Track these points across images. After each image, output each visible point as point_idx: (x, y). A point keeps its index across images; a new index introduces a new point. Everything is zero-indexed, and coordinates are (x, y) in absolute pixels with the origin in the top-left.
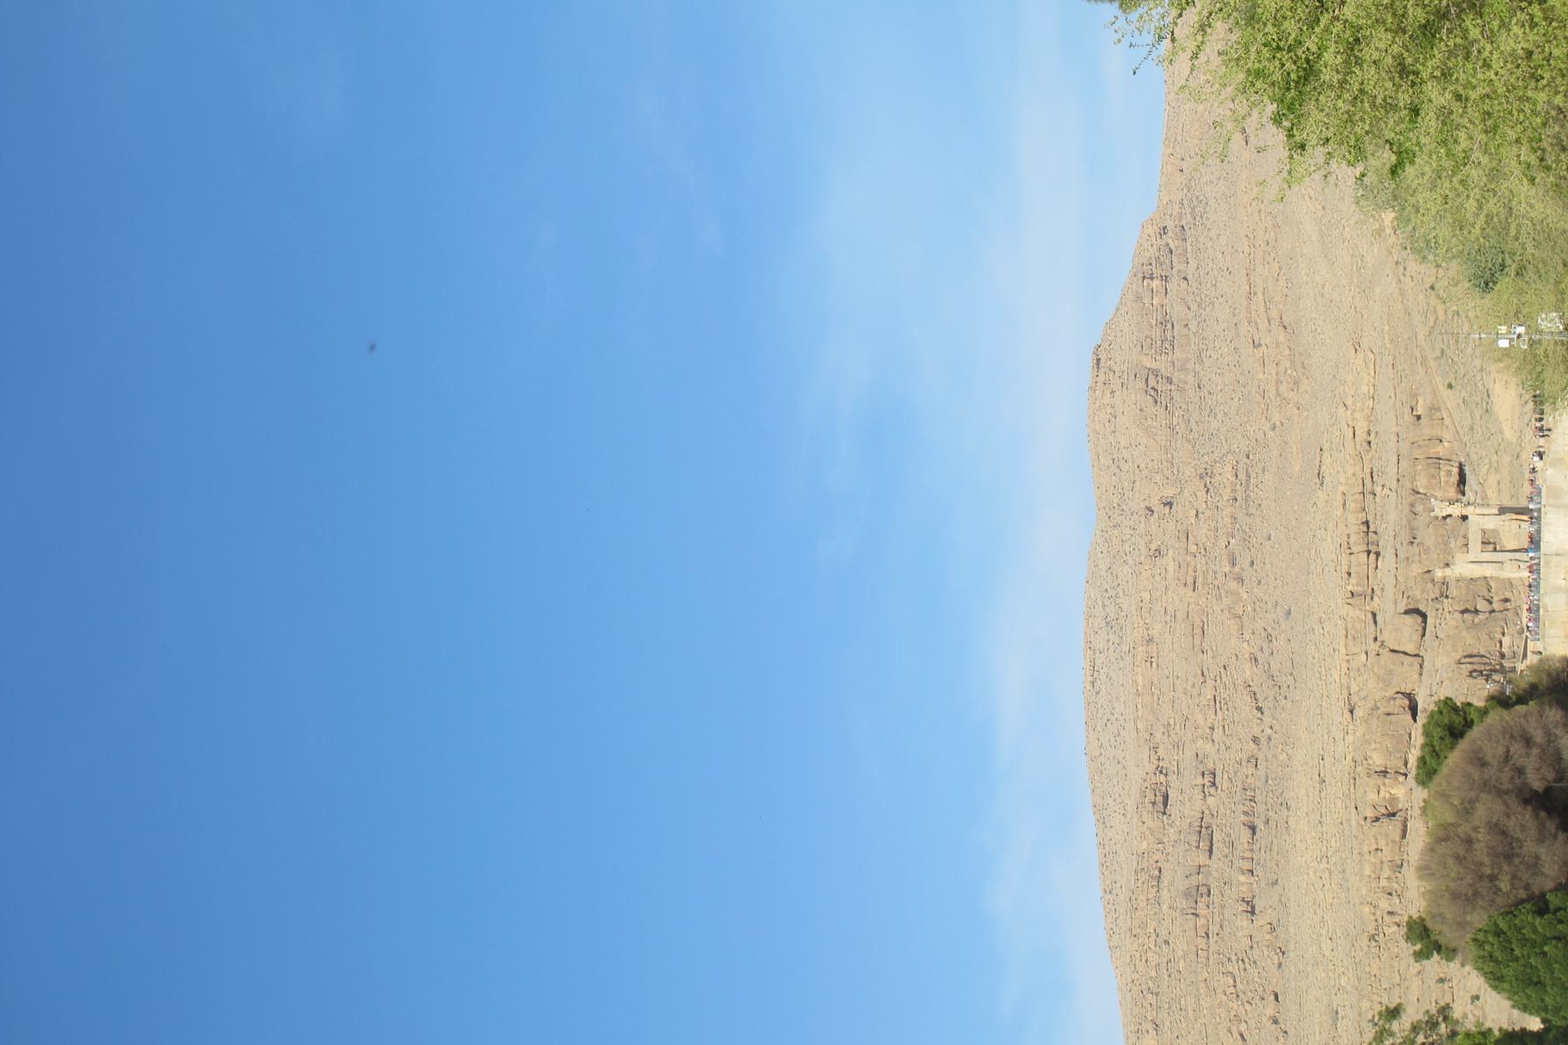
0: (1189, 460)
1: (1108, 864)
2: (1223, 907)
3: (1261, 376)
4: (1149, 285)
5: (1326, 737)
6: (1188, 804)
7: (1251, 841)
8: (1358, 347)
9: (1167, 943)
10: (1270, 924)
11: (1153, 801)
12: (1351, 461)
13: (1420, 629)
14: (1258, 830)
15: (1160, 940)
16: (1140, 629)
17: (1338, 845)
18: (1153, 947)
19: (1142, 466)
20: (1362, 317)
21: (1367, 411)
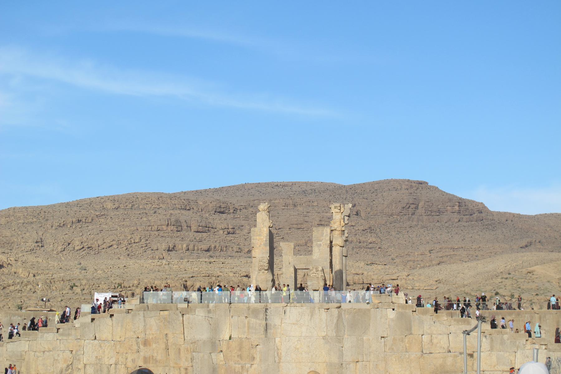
0: (377, 223)
2: (172, 237)
3: (416, 254)
4: (456, 205)
5: (234, 265)
6: (219, 222)
7: (202, 249)
8: (438, 282)
9: (155, 212)
10: (163, 258)
11: (221, 207)
12: (380, 278)
14: (208, 253)
15: (156, 209)
16: (300, 201)
17: (174, 269)
18: (153, 207)
19: (374, 202)
20: (454, 284)
21: (406, 286)
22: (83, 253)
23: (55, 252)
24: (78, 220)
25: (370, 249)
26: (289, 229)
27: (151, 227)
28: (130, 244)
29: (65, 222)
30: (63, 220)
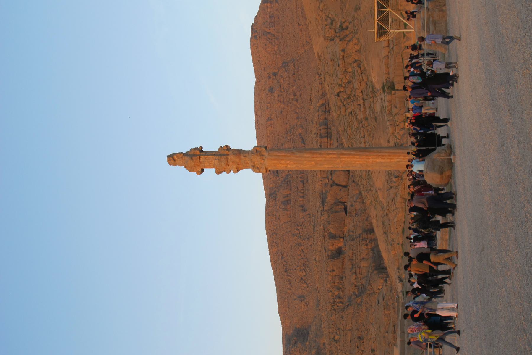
0: (281, 61)
1: (265, 179)
3: (301, 35)
9: (279, 219)
13: (347, 176)
18: (275, 220)
19: (267, 63)
22: (307, 269)
23: (308, 289)
24: (286, 271)
25: (299, 67)
26: (286, 124)
27: (289, 222)
28: (301, 237)
29: (287, 281)
30: (285, 281)
